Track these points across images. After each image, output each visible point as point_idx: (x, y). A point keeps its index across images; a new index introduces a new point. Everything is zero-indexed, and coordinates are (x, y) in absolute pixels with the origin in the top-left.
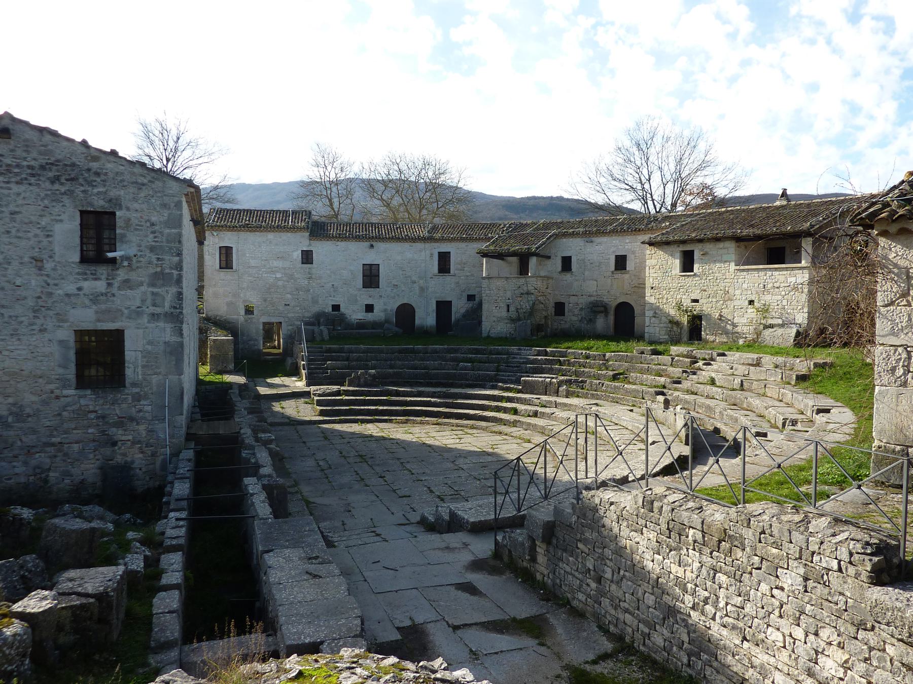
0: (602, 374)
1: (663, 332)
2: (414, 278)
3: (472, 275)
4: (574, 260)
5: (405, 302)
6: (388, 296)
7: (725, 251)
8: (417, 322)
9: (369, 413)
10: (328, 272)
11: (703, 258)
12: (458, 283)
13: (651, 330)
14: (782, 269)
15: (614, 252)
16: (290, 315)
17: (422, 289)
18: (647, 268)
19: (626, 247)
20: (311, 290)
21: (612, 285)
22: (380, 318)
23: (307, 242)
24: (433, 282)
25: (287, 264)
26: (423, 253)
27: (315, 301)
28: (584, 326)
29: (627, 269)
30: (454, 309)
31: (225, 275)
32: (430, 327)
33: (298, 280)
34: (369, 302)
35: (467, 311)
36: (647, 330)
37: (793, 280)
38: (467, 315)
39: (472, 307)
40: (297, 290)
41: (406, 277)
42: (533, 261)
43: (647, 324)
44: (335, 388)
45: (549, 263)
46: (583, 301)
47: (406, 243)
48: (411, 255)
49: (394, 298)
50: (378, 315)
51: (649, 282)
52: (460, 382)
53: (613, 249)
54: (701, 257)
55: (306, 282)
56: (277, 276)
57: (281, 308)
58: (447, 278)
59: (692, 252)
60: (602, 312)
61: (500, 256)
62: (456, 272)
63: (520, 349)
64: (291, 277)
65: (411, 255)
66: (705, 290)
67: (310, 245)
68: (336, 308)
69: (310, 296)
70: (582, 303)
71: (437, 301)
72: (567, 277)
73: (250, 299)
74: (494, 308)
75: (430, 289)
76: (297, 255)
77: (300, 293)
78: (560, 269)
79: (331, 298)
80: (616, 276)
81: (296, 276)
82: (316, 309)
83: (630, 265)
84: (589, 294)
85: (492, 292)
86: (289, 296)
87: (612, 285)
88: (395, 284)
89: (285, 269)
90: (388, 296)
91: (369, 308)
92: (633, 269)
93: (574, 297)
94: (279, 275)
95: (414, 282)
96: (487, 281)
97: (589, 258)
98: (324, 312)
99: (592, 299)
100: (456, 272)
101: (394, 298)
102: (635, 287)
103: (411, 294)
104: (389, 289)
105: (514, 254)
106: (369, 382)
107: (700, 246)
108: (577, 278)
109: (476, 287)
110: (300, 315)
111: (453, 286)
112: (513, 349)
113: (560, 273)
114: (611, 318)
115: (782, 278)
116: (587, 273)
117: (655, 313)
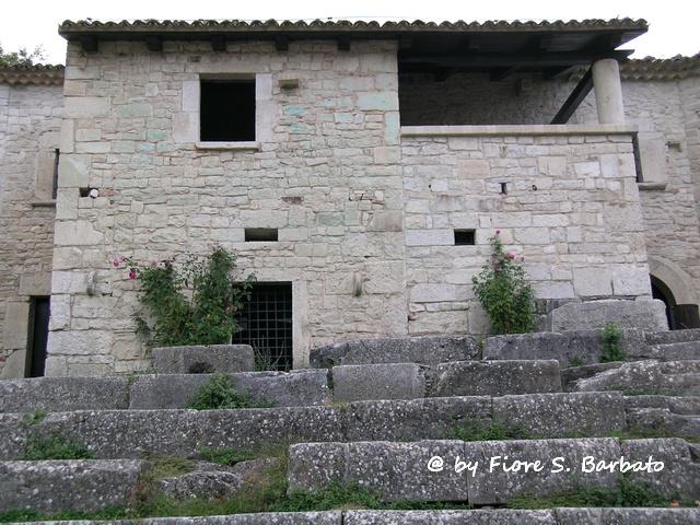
1: (132, 346)
7: (368, 82)
11: (290, 99)
14: (552, 140)
37: (592, 168)
51: (76, 170)
54: (282, 97)
66: (297, 200)
107: (277, 64)
115: (557, 166)
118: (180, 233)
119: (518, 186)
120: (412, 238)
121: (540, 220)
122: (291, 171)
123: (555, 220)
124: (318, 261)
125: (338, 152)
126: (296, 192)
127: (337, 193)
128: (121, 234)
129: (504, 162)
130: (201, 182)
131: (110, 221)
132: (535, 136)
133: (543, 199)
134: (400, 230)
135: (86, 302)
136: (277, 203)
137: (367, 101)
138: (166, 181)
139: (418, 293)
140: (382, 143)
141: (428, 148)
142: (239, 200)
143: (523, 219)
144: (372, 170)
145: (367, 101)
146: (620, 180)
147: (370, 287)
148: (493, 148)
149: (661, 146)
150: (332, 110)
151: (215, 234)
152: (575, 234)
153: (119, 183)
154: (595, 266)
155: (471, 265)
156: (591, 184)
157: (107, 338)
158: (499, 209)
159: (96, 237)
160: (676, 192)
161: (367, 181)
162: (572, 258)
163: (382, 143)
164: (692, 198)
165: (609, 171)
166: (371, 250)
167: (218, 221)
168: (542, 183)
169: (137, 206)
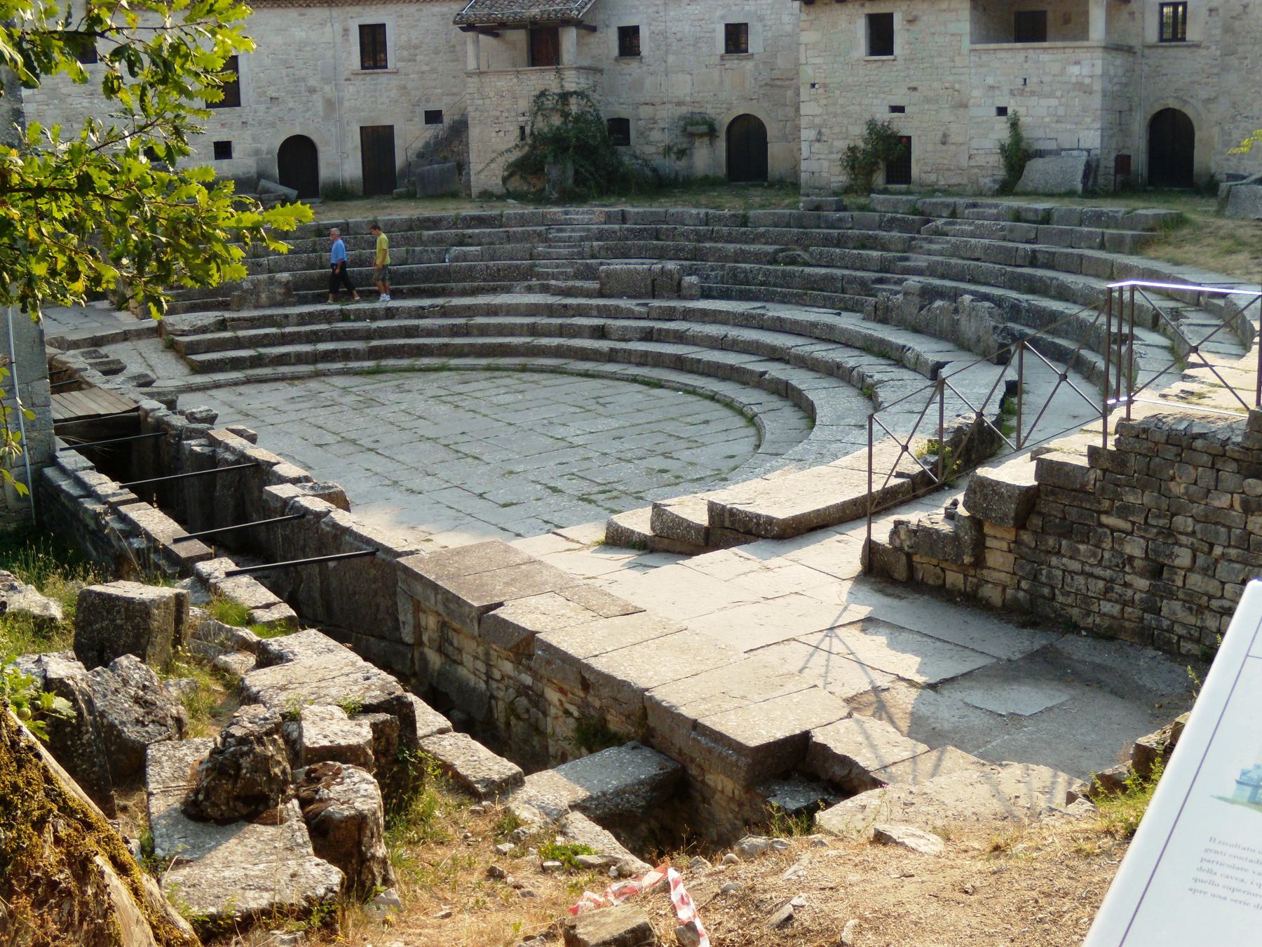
0: (749, 252)
1: (837, 169)
2: (312, 82)
3: (434, 71)
4: (644, 33)
5: (298, 131)
6: (260, 123)
8: (326, 172)
9: (300, 359)
11: (912, 28)
12: (405, 88)
13: (814, 166)
15: (723, 17)
17: (330, 105)
18: (802, 48)
19: (747, 8)
21: (721, 82)
22: (245, 170)
24: (351, 87)
26: (328, 29)
28: (671, 165)
29: (750, 50)
30: (399, 142)
32: (352, 182)
33: (70, 100)
34: (224, 138)
35: (427, 145)
36: (804, 166)
37: (1075, 70)
38: (424, 155)
39: (437, 137)
40: (68, 120)
41: (295, 81)
42: (569, 38)
43: (805, 153)
44: (210, 317)
45: (593, 39)
46: (666, 114)
47: (292, 10)
48: (303, 34)
49: (273, 125)
50: (243, 161)
51: (808, 73)
52: (461, 285)
53: (719, 13)
55: (86, 103)
58: (381, 79)
59: (889, 17)
60: (701, 135)
61: (494, 29)
62: (400, 65)
63: (566, 213)
65: (303, 34)
66: (915, 89)
70: (663, 119)
71: (362, 128)
72: (632, 67)
74: (494, 134)
75: (347, 104)
77: (75, 126)
78: (616, 52)
80: (728, 64)
81: (64, 91)
83: (755, 43)
84: (675, 100)
85: (488, 101)
87: (721, 82)
88: (274, 95)
90: (260, 123)
91: (223, 150)
92: (762, 50)
93: (646, 107)
95: (312, 91)
96: (475, 79)
97: (674, 30)
99: (684, 110)
100: (400, 65)
101: (273, 125)
102: (767, 84)
103: (307, 115)
104: (262, 107)
105: (517, 25)
106: (279, 298)
108: (651, 69)
109: (443, 94)
111: (394, 93)
112: (555, 213)
113: (616, 60)
114: (722, 144)
116: (671, 59)
117: (820, 133)
118: (858, 108)
119: (1033, 81)
120: (973, 112)
121: (1044, 102)
122: (912, 72)
123: (1054, 102)
124: (925, 125)
125: (936, 60)
126: (914, 84)
127: (936, 85)
128: (831, 109)
129: (1026, 66)
130: (867, 79)
131: (825, 102)
132: (1045, 49)
133: (1047, 89)
134: (966, 106)
135: (817, 145)
136: (905, 91)
137: (953, 28)
138: (850, 80)
139: (975, 144)
140: (959, 54)
141: (984, 57)
142: (887, 89)
143: (1033, 101)
144: (954, 71)
145: (953, 28)
146: (1091, 77)
147: (953, 138)
148: (1021, 56)
149: (1204, 12)
150: (933, 34)
151: (874, 109)
152: (1061, 111)
153: (828, 81)
154: (1070, 131)
155: (1001, 130)
156: (1074, 80)
157: (826, 164)
158: (1022, 95)
159: (818, 111)
160: (1208, 48)
161: (951, 78)
162: (1059, 126)
163: (959, 54)
164: (1218, 53)
165: (1086, 71)
166: (952, 119)
167: (875, 101)
168: (1047, 79)
169: (837, 92)
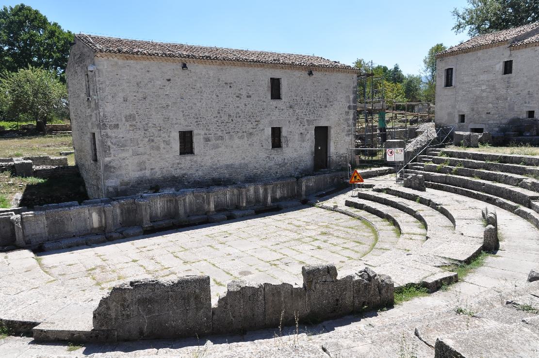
10: (525, 79)
16: (490, 122)
20: (509, 99)
23: (509, 52)
25: (491, 76)
27: (511, 109)
31: (449, 91)
56: (483, 88)
57: (484, 116)
64: (494, 87)
67: (511, 55)
68: (531, 114)
69: (507, 104)
73: (463, 110)
76: (500, 67)
79: (526, 105)
82: (511, 116)
86: (490, 105)
89: (488, 81)
94: (484, 87)
98: (519, 119)
110: (498, 122)
